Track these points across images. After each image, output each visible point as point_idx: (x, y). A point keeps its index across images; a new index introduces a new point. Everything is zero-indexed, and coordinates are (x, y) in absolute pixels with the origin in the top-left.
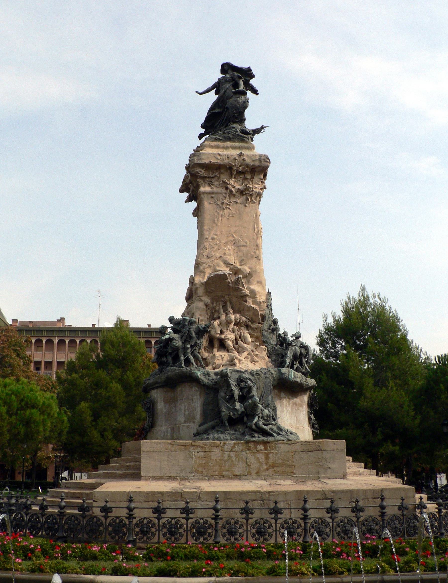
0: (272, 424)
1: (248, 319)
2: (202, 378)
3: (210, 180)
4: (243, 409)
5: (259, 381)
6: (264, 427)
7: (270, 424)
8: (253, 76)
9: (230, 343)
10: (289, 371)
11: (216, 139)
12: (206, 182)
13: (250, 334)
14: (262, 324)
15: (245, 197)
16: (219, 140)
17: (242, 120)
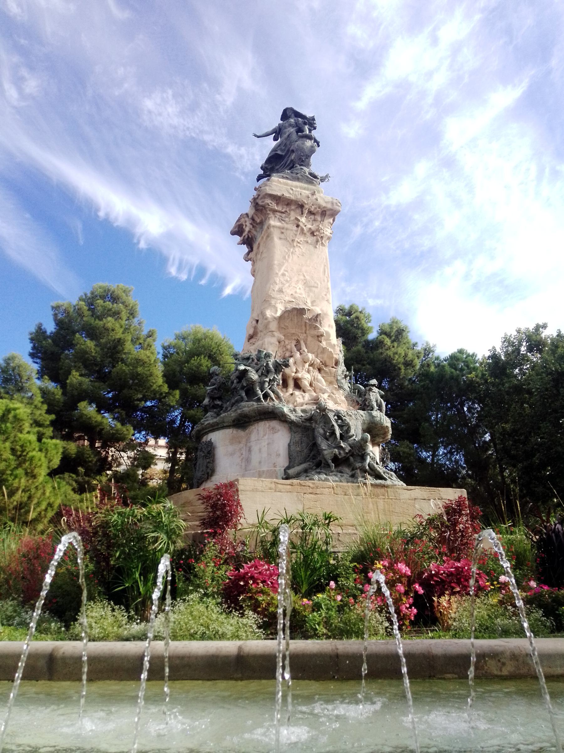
9: (306, 383)
13: (323, 377)
15: (315, 237)
16: (287, 178)
17: (308, 165)
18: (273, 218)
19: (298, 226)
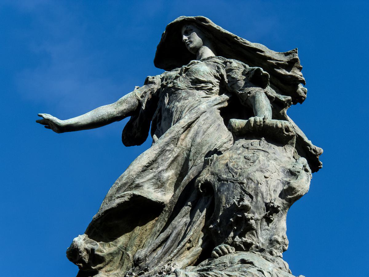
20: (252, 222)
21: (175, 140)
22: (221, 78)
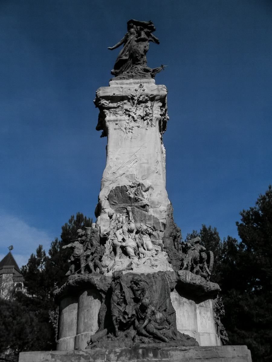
0: (166, 328)
1: (150, 228)
2: (98, 283)
3: (114, 109)
4: (134, 313)
5: (156, 284)
6: (155, 331)
7: (163, 328)
8: (154, 30)
9: (130, 250)
10: (186, 273)
11: (121, 78)
12: (111, 111)
14: (163, 232)
18: (109, 114)
19: (129, 116)
20: (139, 59)
21: (127, 46)
22: (136, 31)
